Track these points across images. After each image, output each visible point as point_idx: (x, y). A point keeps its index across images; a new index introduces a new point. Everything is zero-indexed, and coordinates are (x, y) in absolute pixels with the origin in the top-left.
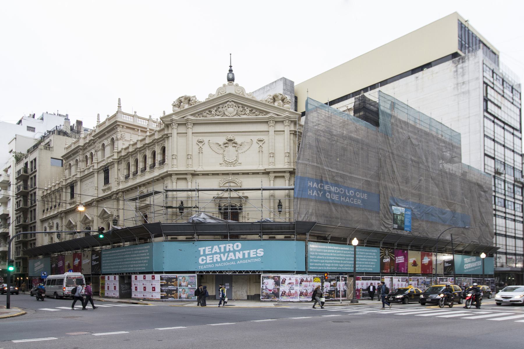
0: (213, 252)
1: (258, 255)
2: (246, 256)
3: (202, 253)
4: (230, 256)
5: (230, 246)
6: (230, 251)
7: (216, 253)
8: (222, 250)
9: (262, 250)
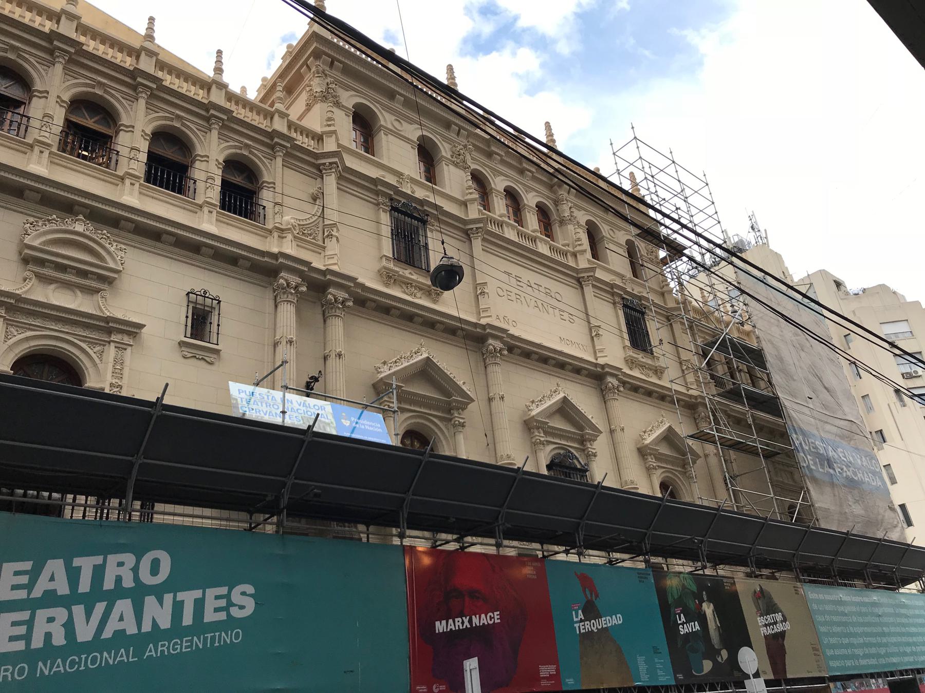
0: (37, 593)
1: (235, 612)
4: (115, 615)
6: (119, 592)
7: (51, 599)
8: (84, 586)
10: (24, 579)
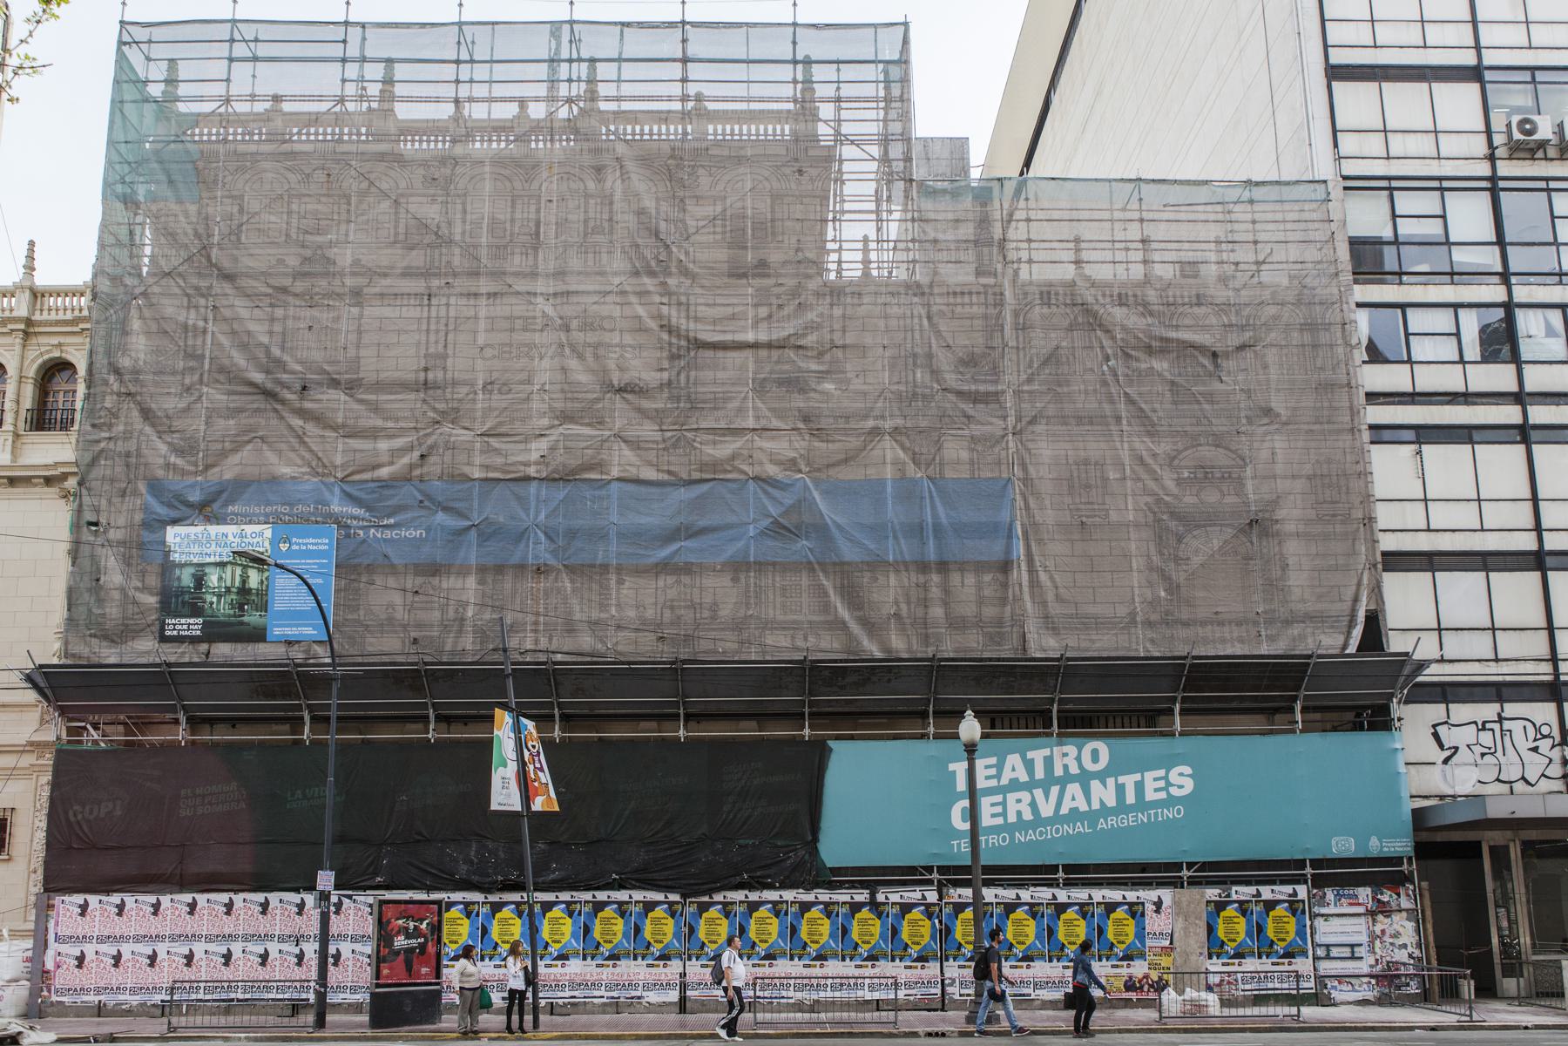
0: (1004, 781)
1: (1174, 791)
2: (1130, 798)
4: (1067, 796)
5: (1070, 755)
6: (1067, 779)
7: (1015, 785)
8: (1040, 774)
9: (1187, 770)
10: (993, 771)
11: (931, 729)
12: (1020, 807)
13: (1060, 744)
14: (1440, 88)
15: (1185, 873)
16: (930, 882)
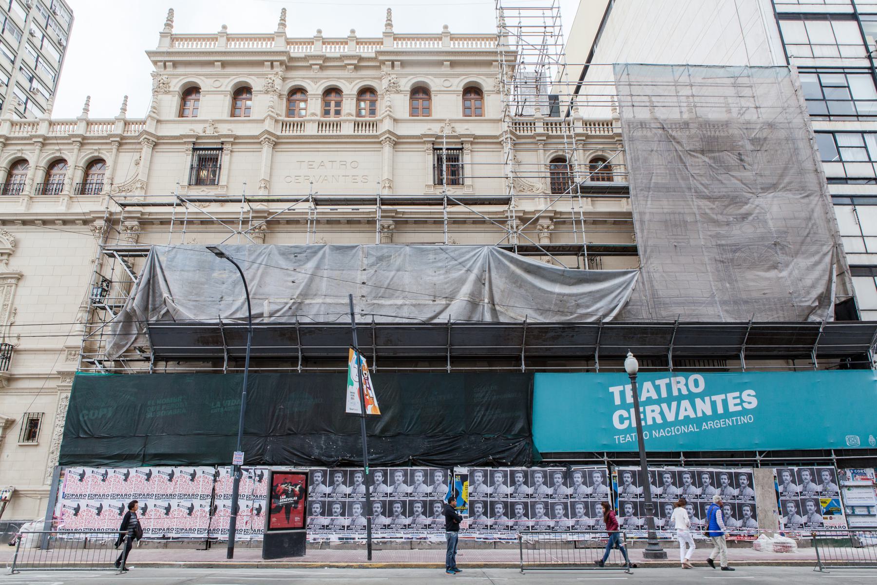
1: (746, 405)
2: (720, 410)
3: (618, 401)
5: (680, 383)
6: (680, 398)
8: (664, 394)
9: (752, 392)
11: (597, 366)
12: (653, 414)
13: (676, 376)
14: (836, 24)
15: (758, 458)
16: (602, 463)
